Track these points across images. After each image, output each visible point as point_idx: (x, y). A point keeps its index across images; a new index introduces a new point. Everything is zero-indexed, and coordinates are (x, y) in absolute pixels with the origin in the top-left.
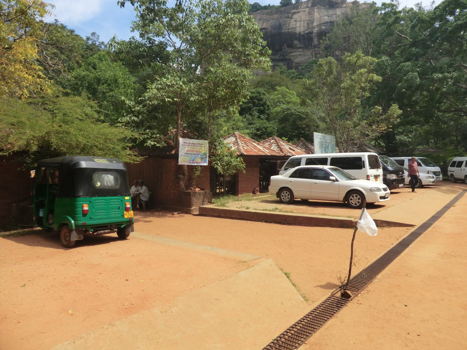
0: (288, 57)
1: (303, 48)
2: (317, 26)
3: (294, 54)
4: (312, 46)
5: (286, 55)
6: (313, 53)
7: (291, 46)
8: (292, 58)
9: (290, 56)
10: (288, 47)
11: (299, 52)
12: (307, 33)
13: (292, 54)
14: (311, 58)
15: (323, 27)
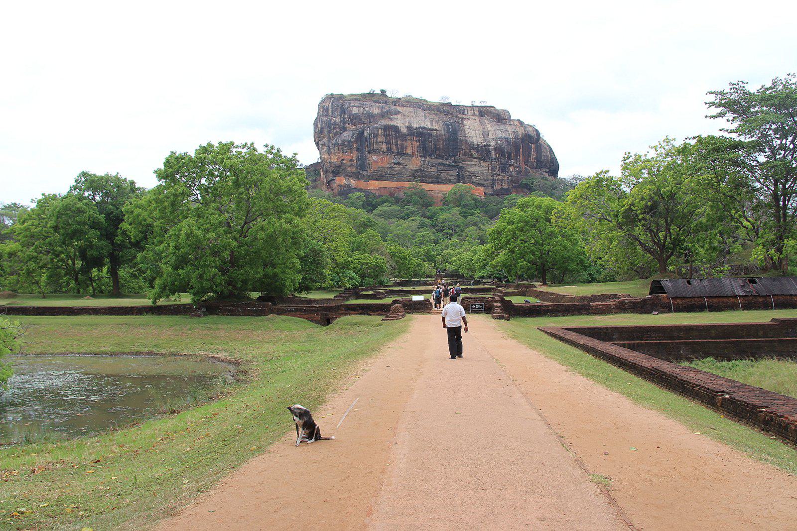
0: (461, 165)
3: (469, 163)
5: (459, 162)
9: (463, 164)
12: (485, 145)
13: (466, 163)
15: (499, 142)
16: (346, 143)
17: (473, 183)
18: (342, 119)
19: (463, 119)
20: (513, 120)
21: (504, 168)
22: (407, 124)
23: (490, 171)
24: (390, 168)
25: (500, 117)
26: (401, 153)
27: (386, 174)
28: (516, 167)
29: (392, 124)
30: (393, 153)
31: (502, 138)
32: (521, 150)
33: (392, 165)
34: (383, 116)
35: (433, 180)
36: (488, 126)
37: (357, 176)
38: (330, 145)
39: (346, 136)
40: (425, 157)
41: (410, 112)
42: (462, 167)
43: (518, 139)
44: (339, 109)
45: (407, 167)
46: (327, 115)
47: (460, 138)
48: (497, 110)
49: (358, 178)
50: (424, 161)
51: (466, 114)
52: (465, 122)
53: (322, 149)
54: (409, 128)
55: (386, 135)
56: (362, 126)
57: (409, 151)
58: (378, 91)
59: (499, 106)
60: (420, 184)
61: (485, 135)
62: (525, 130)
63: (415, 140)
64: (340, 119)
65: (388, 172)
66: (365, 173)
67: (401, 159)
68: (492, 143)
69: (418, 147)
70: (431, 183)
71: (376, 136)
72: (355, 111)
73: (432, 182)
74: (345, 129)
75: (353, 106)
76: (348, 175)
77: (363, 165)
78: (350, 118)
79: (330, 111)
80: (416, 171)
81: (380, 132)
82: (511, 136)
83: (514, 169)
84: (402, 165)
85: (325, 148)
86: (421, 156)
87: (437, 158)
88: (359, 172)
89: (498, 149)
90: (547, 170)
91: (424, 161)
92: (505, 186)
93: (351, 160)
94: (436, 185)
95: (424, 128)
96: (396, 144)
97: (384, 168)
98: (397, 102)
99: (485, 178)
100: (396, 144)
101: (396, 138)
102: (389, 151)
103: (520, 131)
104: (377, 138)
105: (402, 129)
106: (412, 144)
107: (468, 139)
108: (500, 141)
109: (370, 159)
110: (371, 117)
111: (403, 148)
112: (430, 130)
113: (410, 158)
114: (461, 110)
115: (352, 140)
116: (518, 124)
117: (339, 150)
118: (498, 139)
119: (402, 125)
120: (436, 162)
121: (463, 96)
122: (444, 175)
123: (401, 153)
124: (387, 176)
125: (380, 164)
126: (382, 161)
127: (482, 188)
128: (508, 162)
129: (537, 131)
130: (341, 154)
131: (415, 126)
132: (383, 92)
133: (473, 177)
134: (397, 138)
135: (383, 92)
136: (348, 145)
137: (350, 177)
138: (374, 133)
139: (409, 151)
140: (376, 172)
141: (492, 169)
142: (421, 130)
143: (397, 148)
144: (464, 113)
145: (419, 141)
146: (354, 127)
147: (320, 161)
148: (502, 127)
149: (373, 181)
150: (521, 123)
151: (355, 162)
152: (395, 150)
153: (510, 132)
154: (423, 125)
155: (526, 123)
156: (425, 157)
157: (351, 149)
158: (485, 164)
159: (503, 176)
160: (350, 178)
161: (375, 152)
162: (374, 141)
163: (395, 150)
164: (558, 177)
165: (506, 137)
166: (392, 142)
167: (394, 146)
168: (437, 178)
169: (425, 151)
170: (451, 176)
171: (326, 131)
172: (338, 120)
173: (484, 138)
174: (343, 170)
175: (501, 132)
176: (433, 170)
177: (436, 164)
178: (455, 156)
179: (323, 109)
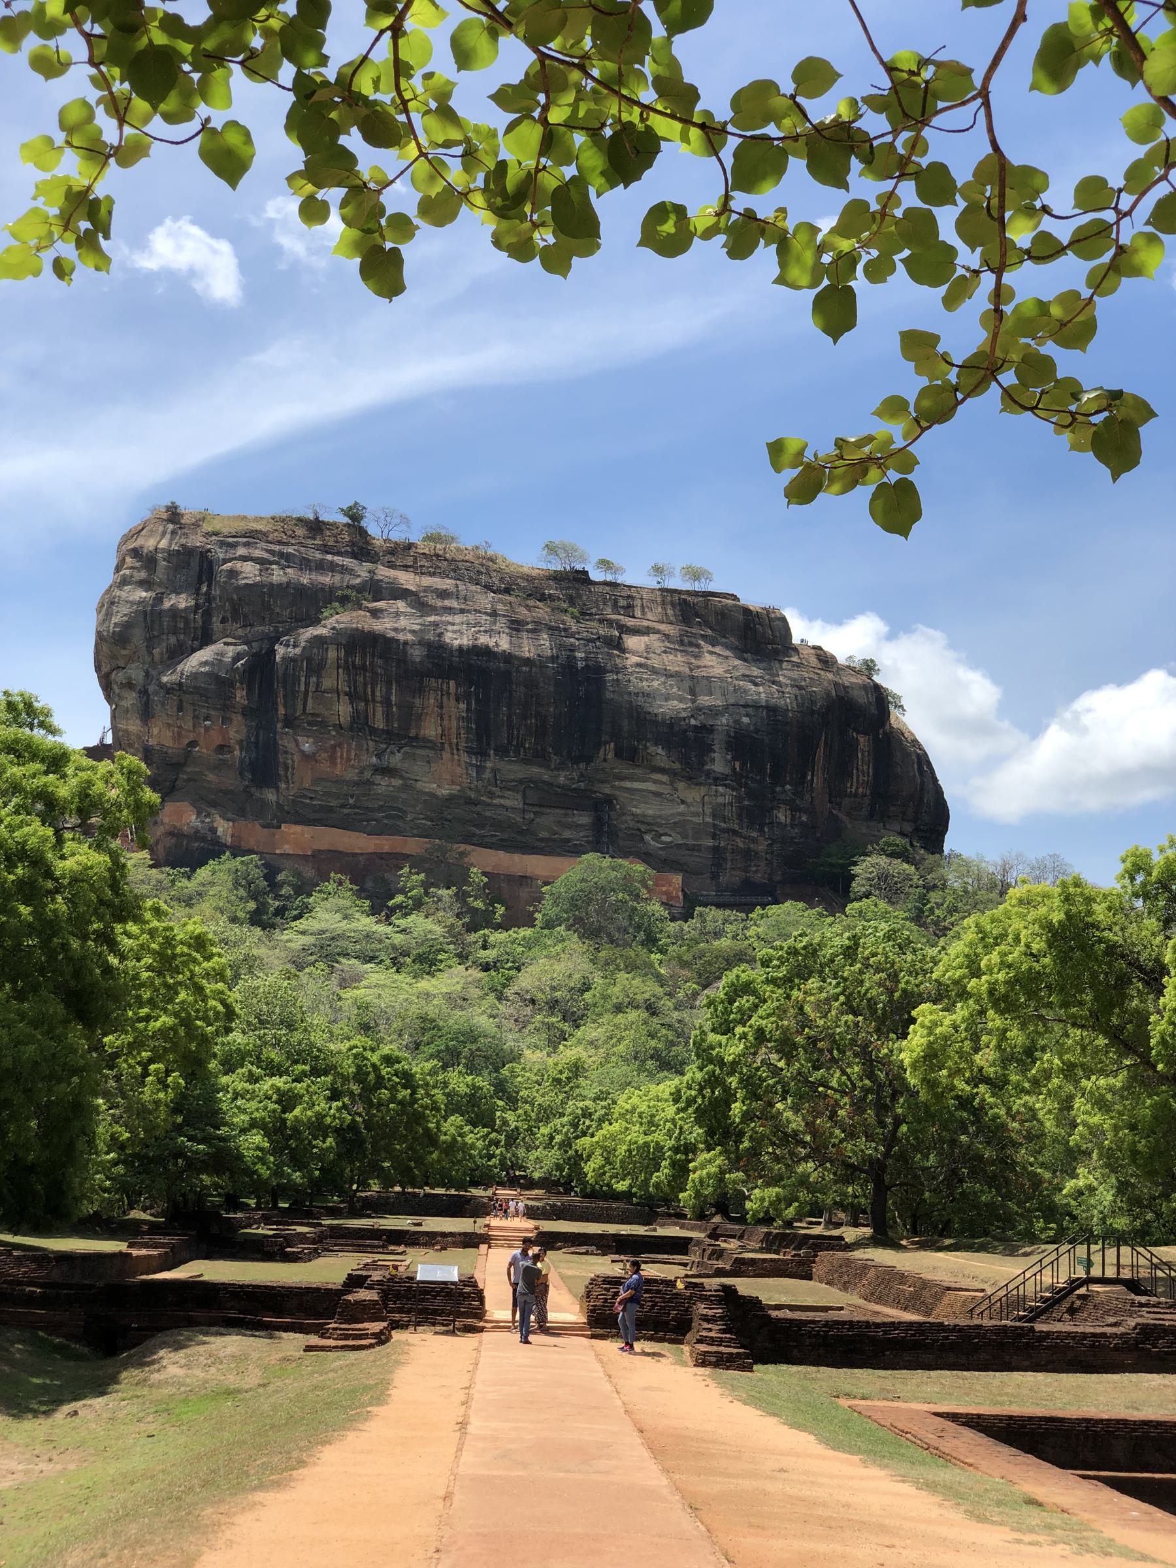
0: (608, 791)
1: (675, 774)
2: (727, 707)
7: (628, 754)
8: (623, 796)
10: (618, 754)
11: (655, 782)
12: (695, 726)
13: (628, 784)
14: (697, 814)
15: (745, 720)
17: (646, 857)
19: (624, 629)
21: (755, 813)
22: (431, 636)
23: (709, 820)
24: (357, 784)
26: (401, 734)
27: (343, 806)
28: (800, 810)
30: (373, 731)
31: (756, 706)
32: (821, 752)
33: (367, 775)
35: (506, 836)
37: (239, 806)
38: (152, 688)
40: (482, 754)
41: (443, 594)
42: (609, 800)
43: (813, 712)
45: (419, 785)
47: (609, 695)
48: (746, 611)
49: (241, 813)
50: (480, 769)
51: (638, 613)
52: (632, 642)
53: (121, 698)
55: (350, 669)
56: (267, 629)
57: (430, 730)
58: (333, 516)
59: (753, 598)
60: (463, 847)
63: (452, 690)
65: (351, 801)
66: (271, 796)
72: (250, 572)
74: (206, 639)
75: (244, 559)
76: (206, 802)
77: (264, 766)
78: (231, 600)
80: (450, 799)
81: (332, 654)
82: (787, 701)
83: (793, 817)
84: (402, 778)
85: (130, 699)
86: (470, 751)
87: (526, 762)
88: (246, 790)
89: (739, 743)
90: (908, 827)
91: (480, 769)
92: (759, 875)
93: (221, 748)
94: (517, 857)
96: (387, 702)
97: (339, 781)
98: (399, 553)
99: (690, 842)
100: (387, 702)
101: (389, 683)
104: (319, 677)
105: (410, 651)
106: (441, 707)
108: (747, 715)
109: (291, 746)
111: (410, 716)
112: (508, 658)
113: (431, 754)
114: (622, 598)
116: (814, 661)
117: (180, 709)
118: (743, 711)
120: (520, 776)
122: (548, 821)
124: (346, 811)
125: (325, 766)
126: (332, 759)
127: (677, 879)
128: (775, 792)
129: (877, 688)
130: (188, 724)
132: (354, 515)
133: (648, 837)
134: (389, 683)
135: (354, 515)
136: (214, 689)
137: (213, 804)
138: (309, 660)
139: (430, 730)
140: (305, 797)
143: (388, 717)
144: (629, 610)
145: (466, 697)
147: (109, 740)
149: (298, 829)
150: (826, 660)
151: (237, 753)
152: (380, 724)
154: (483, 640)
155: (841, 660)
156: (482, 754)
157: (225, 708)
158: (693, 794)
159: (754, 841)
160: (213, 811)
161: (310, 723)
162: (307, 684)
163: (380, 724)
164: (946, 849)
167: (380, 710)
168: (521, 832)
169: (483, 738)
170: (570, 827)
173: (694, 701)
174: (189, 780)
175: (756, 684)
176: (507, 803)
177: (521, 781)
178: (589, 760)
179: (138, 560)
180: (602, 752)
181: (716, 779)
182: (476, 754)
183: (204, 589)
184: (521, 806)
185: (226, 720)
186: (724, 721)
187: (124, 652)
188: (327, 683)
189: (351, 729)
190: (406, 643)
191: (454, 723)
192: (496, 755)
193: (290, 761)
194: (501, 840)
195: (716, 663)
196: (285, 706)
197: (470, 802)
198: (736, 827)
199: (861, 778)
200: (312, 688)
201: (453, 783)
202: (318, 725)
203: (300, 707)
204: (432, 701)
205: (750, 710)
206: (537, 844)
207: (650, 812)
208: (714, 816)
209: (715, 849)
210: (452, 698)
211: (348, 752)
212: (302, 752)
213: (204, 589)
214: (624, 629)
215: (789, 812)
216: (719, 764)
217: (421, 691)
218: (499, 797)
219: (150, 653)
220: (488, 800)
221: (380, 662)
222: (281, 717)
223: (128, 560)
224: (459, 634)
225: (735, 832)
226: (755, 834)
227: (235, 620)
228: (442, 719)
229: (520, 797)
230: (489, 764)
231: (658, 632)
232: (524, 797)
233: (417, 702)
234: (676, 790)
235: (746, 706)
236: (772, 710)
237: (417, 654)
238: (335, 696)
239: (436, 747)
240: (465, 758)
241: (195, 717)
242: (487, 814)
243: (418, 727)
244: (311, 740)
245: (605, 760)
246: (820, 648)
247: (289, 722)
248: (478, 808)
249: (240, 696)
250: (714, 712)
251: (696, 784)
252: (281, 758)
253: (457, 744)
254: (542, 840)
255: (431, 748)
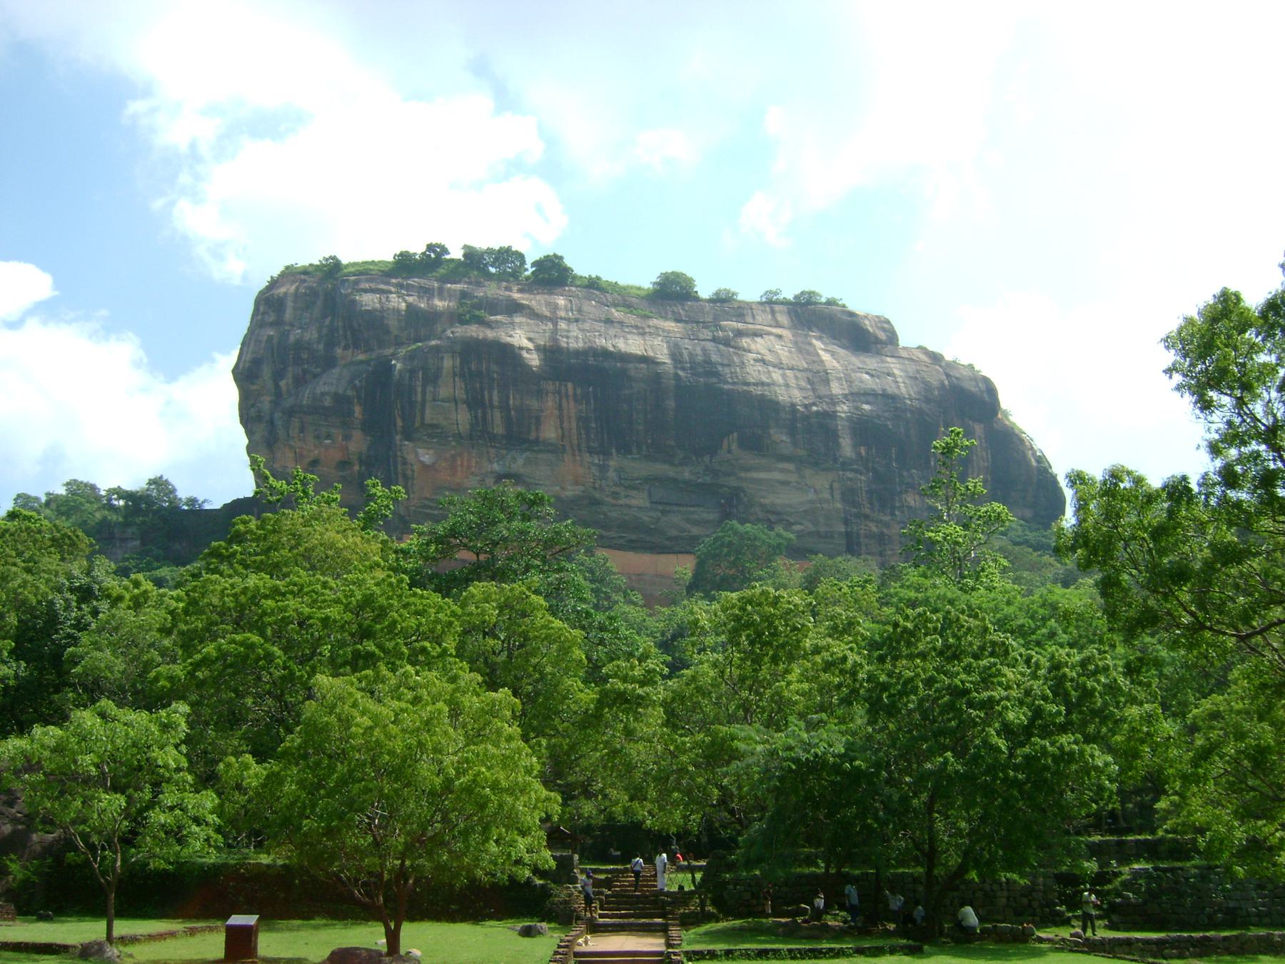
0: (732, 482)
2: (845, 396)
3: (762, 475)
4: (835, 460)
6: (836, 485)
7: (755, 444)
10: (742, 445)
11: (782, 471)
12: (817, 412)
13: (755, 475)
15: (866, 407)
16: (328, 402)
18: (325, 331)
19: (740, 334)
20: (904, 348)
23: (839, 505)
25: (862, 336)
26: (519, 436)
29: (490, 334)
30: (493, 438)
34: (458, 318)
35: (633, 537)
36: (826, 357)
38: (277, 415)
39: (330, 383)
40: (605, 453)
42: (736, 494)
44: (320, 303)
46: (278, 323)
48: (852, 314)
54: (551, 353)
61: (818, 377)
62: (948, 375)
63: (571, 392)
64: (319, 332)
67: (520, 461)
68: (843, 409)
69: (579, 419)
70: (633, 549)
71: (433, 378)
73: (632, 546)
74: (330, 362)
75: (366, 291)
79: (288, 315)
81: (448, 363)
85: (261, 430)
86: (591, 451)
89: (863, 429)
90: (1028, 514)
91: (603, 468)
95: (606, 354)
96: (505, 407)
99: (823, 529)
100: (505, 407)
102: (479, 435)
103: (935, 377)
105: (525, 354)
106: (560, 408)
107: (758, 391)
108: (867, 403)
109: (410, 457)
110: (419, 322)
115: (349, 393)
117: (302, 430)
119: (526, 343)
121: (742, 261)
123: (519, 436)
131: (573, 345)
139: (550, 432)
141: (849, 496)
142: (591, 361)
143: (508, 421)
146: (361, 357)
148: (872, 362)
150: (936, 358)
151: (357, 468)
152: (499, 430)
153: (900, 380)
156: (605, 453)
158: (821, 481)
159: (887, 525)
162: (424, 393)
165: (890, 391)
166: (491, 400)
167: (497, 415)
170: (697, 523)
171: (267, 371)
172: (311, 335)
173: (814, 390)
175: (872, 376)
176: (634, 502)
177: (647, 480)
180: (725, 442)
181: (843, 464)
182: (598, 453)
183: (328, 321)
184: (648, 505)
185: (347, 437)
186: (845, 408)
187: (255, 387)
188: (444, 392)
189: (471, 438)
190: (521, 348)
191: (574, 424)
192: (618, 452)
193: (409, 472)
194: (631, 541)
195: (830, 356)
196: (403, 420)
197: (595, 502)
198: (867, 511)
199: (982, 464)
200: (429, 397)
201: (577, 483)
202: (437, 434)
203: (418, 419)
204: (550, 404)
205: (870, 399)
206: (667, 543)
207: (779, 501)
208: (844, 500)
209: (848, 535)
210: (571, 399)
211: (469, 460)
212: (421, 462)
213: (328, 321)
214: (740, 334)
215: (917, 497)
216: (847, 447)
217: (540, 394)
218: (626, 497)
219: (277, 386)
220: (614, 502)
221: (494, 367)
222: (399, 429)
223: (262, 309)
224: (574, 338)
225: (867, 517)
226: (887, 518)
227: (356, 346)
228: (562, 423)
229: (645, 495)
230: (612, 463)
231: (769, 334)
232: (650, 495)
233: (534, 403)
234: (803, 477)
235: (866, 394)
236: (888, 398)
237: (534, 360)
238: (453, 405)
239: (555, 450)
240: (587, 457)
241: (317, 437)
242: (614, 514)
243: (537, 429)
244: (431, 452)
245: (729, 451)
246: (922, 349)
247: (408, 436)
248: (605, 509)
249: (357, 410)
250: (833, 400)
251: (823, 470)
252: (399, 468)
253: (579, 445)
254: (670, 539)
255: (551, 452)
